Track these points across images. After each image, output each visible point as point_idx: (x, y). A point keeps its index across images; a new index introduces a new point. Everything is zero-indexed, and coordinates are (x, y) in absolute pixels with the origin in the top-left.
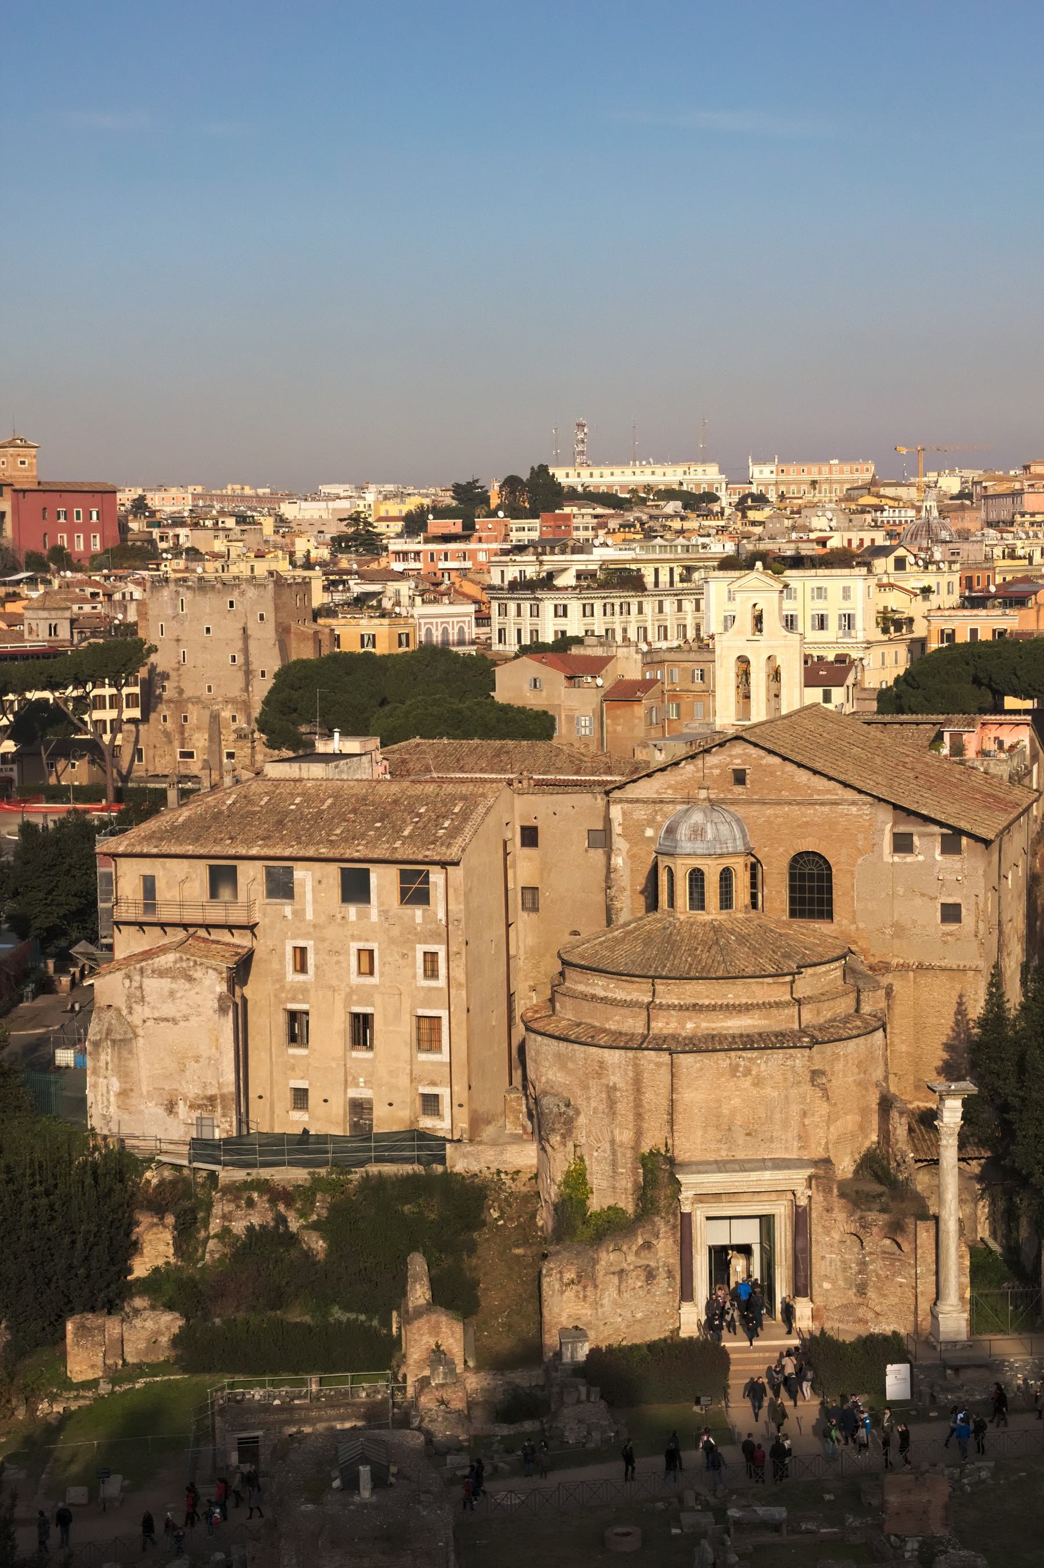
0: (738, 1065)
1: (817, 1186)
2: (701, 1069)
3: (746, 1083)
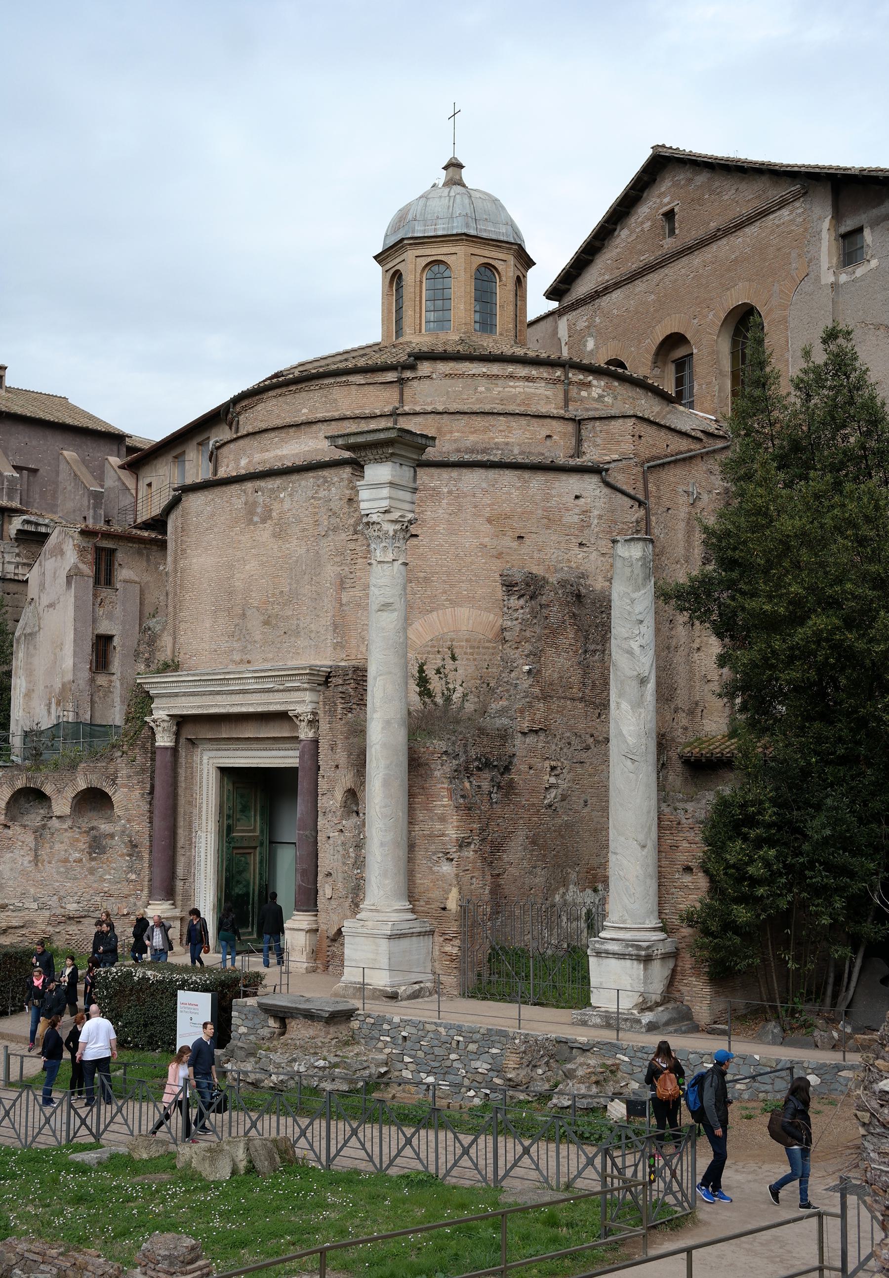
0: (255, 504)
2: (213, 515)
3: (264, 533)
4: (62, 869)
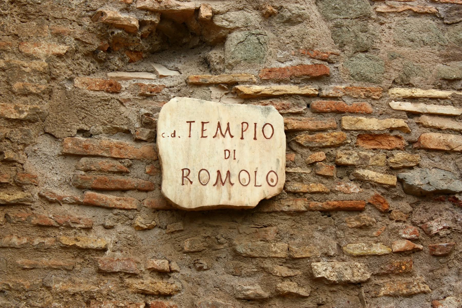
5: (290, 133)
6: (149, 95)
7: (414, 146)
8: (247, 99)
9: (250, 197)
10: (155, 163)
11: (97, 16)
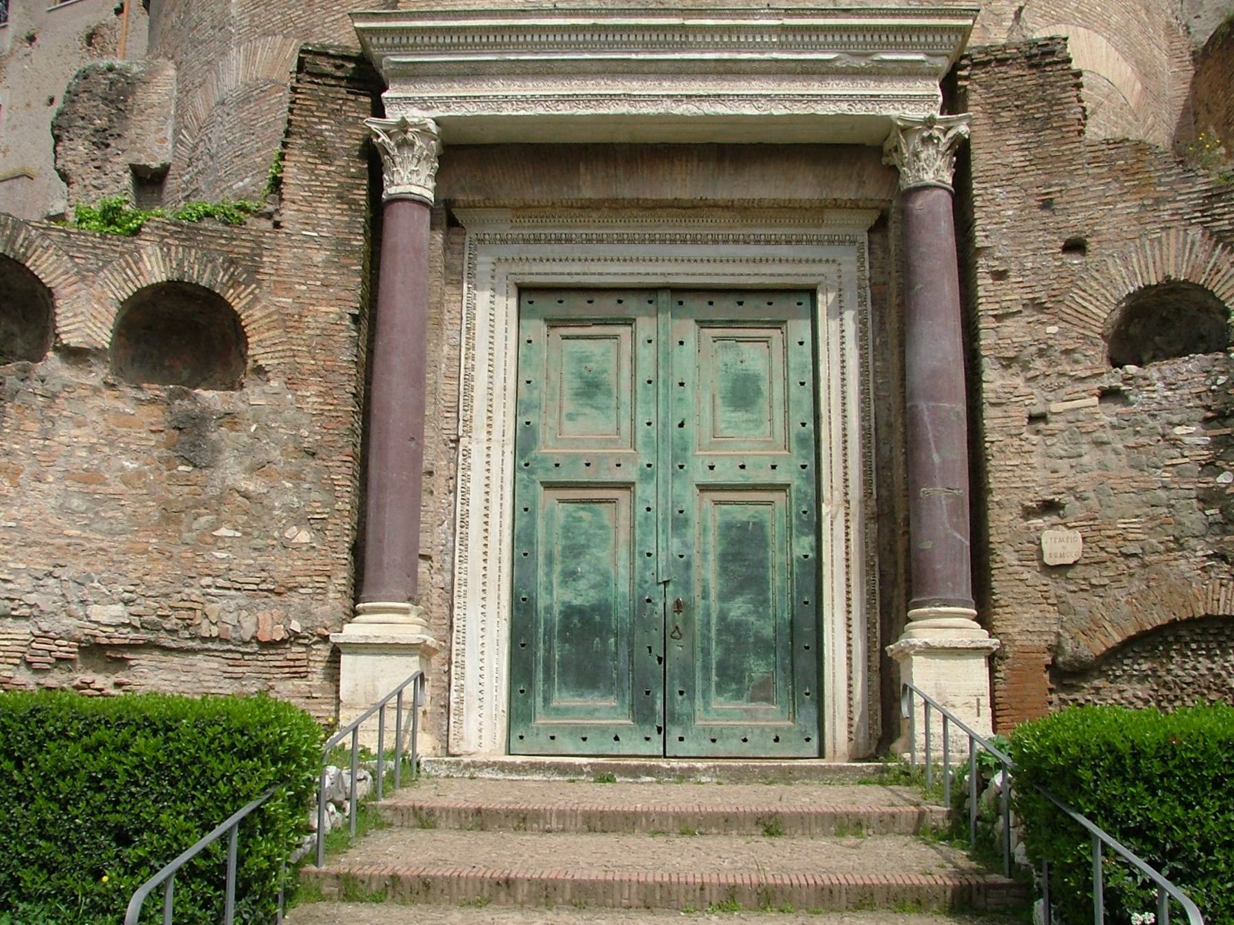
1: (993, 110)
4: (76, 503)
5: (1084, 538)
6: (1038, 529)
7: (1125, 539)
8: (1070, 528)
9: (1071, 561)
10: (1040, 551)
11: (1022, 505)
